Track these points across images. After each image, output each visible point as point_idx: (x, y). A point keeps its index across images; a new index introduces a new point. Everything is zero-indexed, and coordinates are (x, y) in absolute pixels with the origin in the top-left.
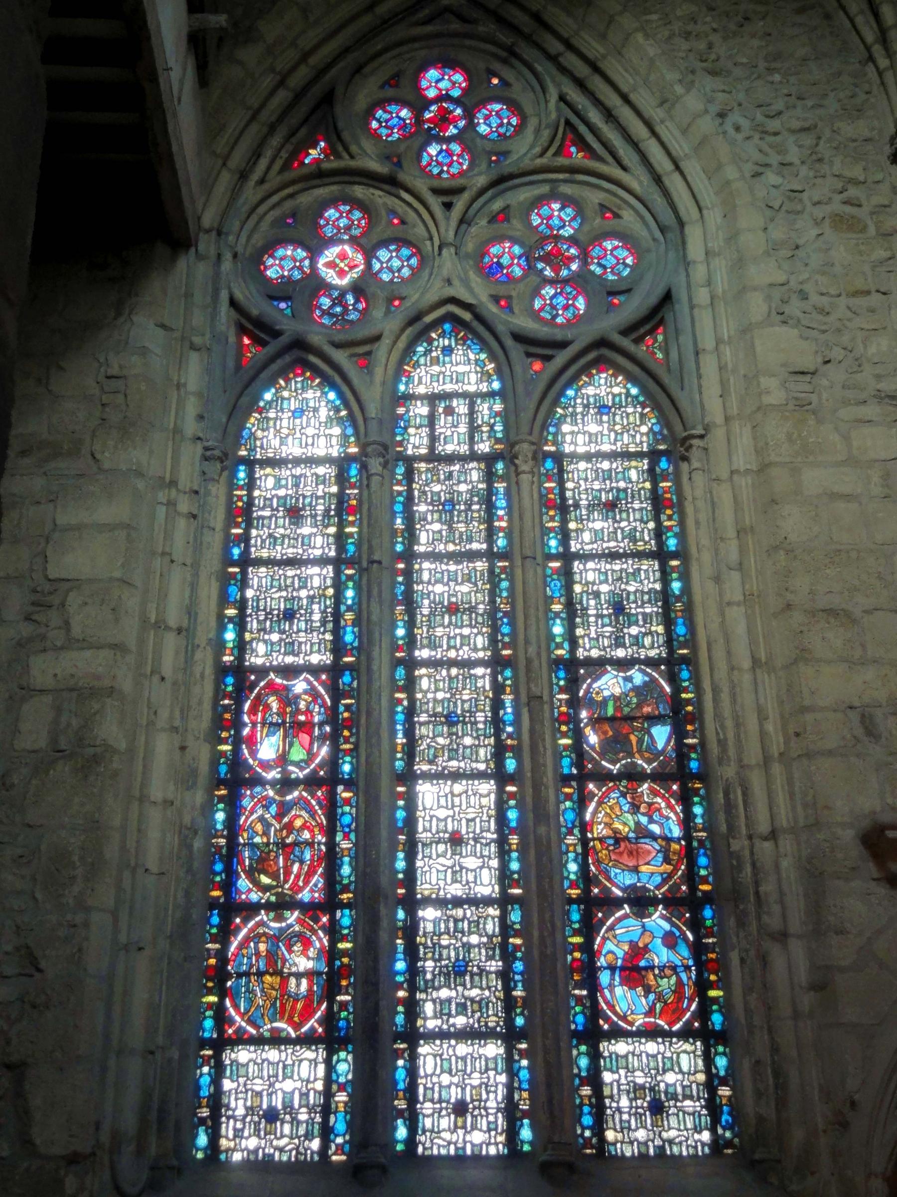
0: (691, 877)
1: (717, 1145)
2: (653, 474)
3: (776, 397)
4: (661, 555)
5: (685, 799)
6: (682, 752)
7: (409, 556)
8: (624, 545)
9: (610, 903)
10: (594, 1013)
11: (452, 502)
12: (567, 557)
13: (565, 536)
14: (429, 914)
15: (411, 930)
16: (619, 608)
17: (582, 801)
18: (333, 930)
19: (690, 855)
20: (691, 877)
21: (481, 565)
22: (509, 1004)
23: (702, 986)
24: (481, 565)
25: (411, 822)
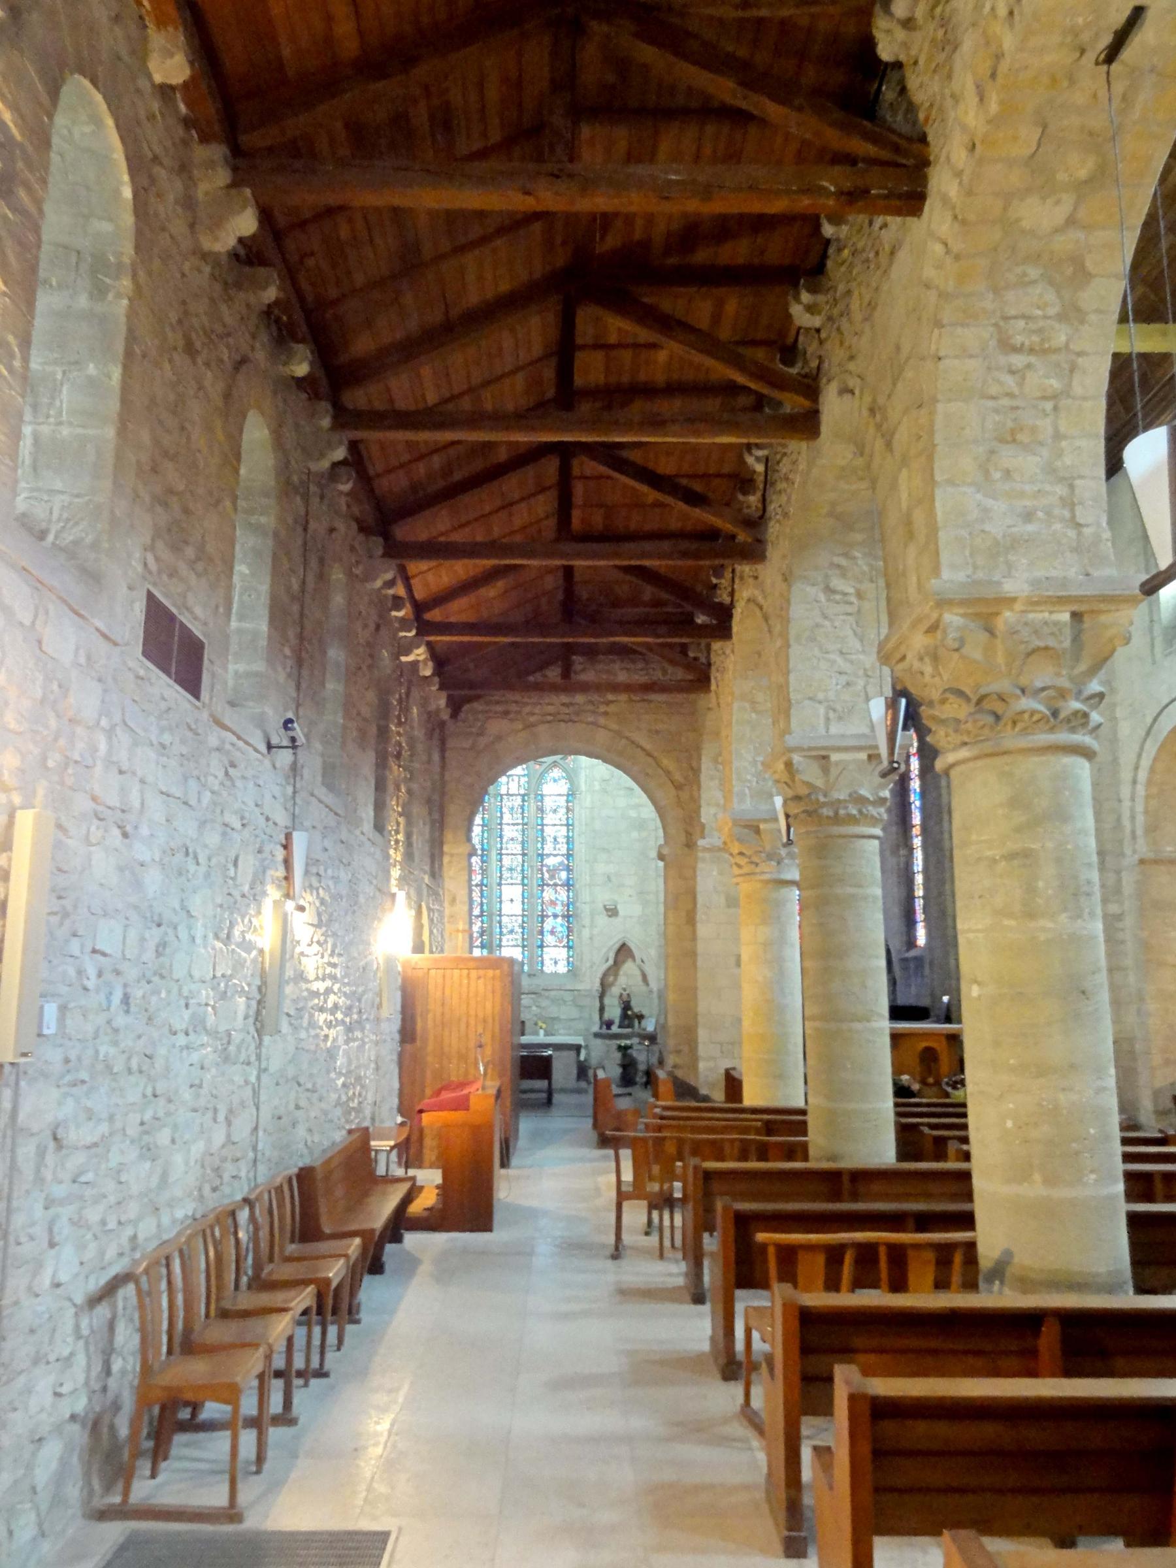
0: (568, 910)
1: (569, 971)
2: (567, 802)
3: (597, 787)
4: (568, 825)
5: (568, 891)
6: (568, 879)
7: (501, 824)
8: (558, 822)
9: (548, 916)
10: (542, 941)
11: (512, 808)
12: (543, 825)
13: (542, 818)
14: (505, 919)
15: (500, 922)
16: (555, 839)
17: (543, 891)
18: (482, 922)
19: (568, 905)
20: (568, 910)
21: (520, 827)
22: (523, 939)
23: (568, 936)
24: (520, 827)
25: (500, 897)
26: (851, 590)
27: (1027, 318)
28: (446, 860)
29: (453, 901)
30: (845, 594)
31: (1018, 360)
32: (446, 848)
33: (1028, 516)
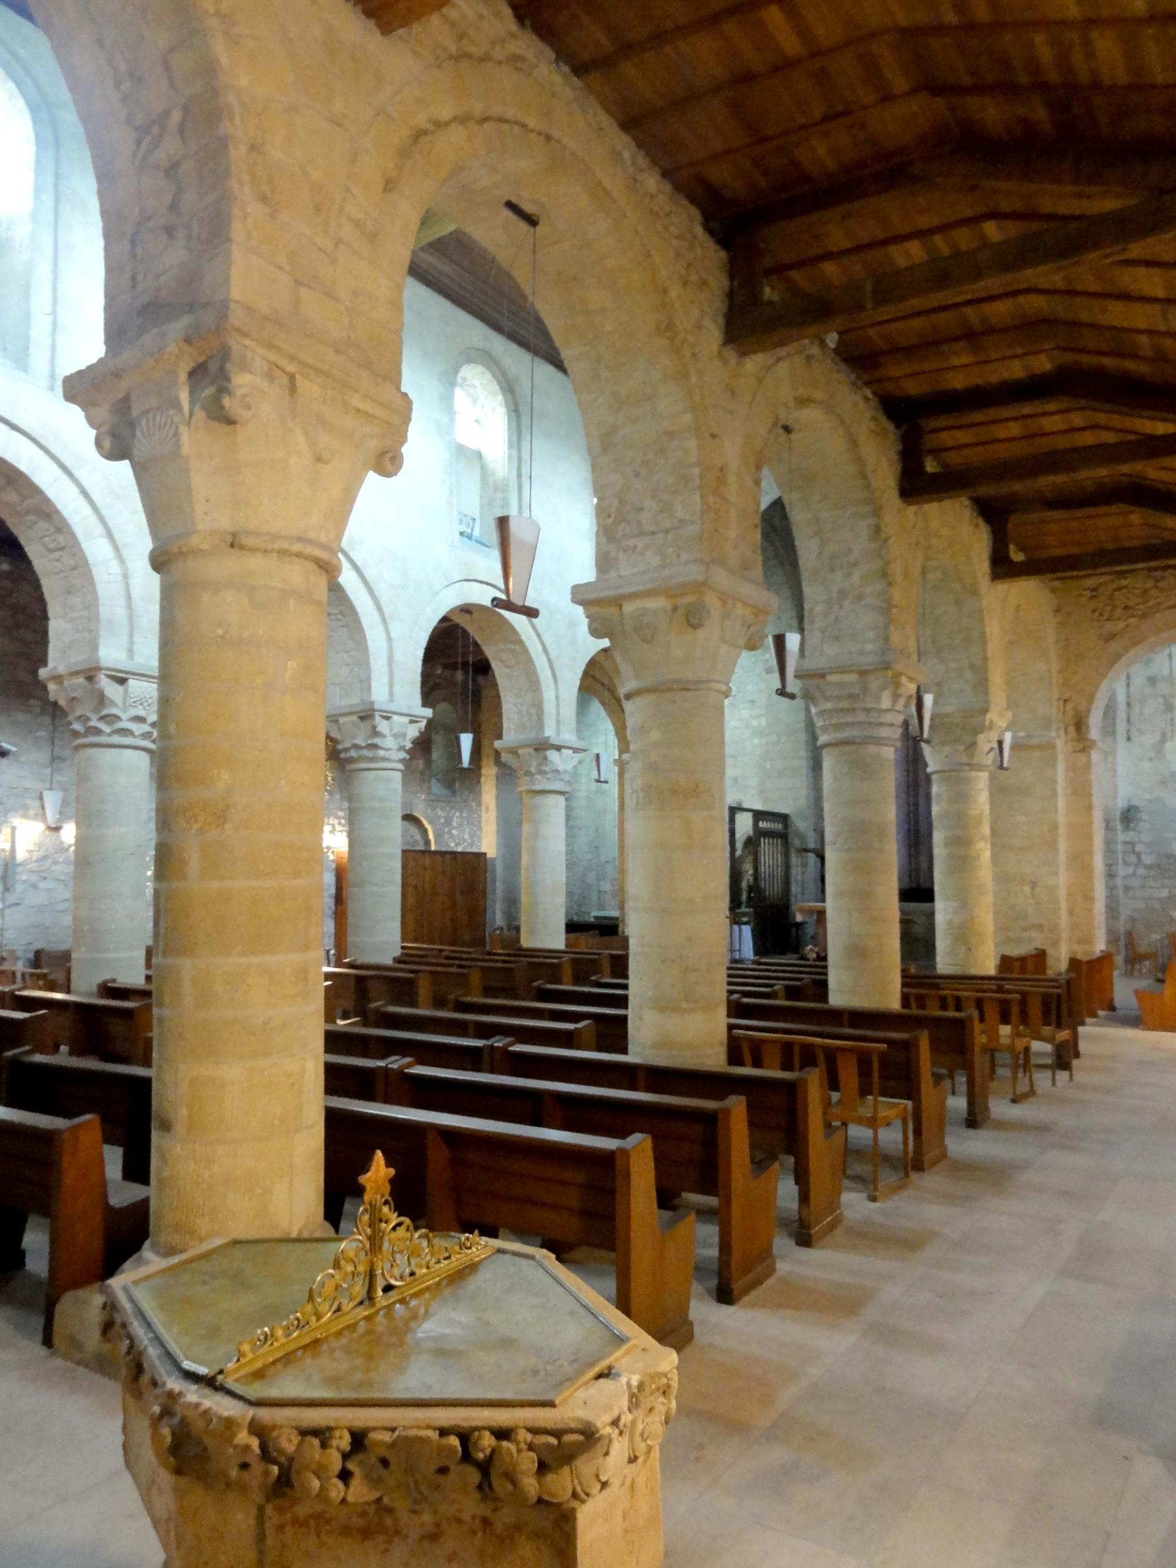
26: (336, 612)
27: (48, 536)
28: (483, 779)
29: (487, 810)
30: (335, 615)
31: (56, 555)
32: (483, 771)
33: (77, 630)
